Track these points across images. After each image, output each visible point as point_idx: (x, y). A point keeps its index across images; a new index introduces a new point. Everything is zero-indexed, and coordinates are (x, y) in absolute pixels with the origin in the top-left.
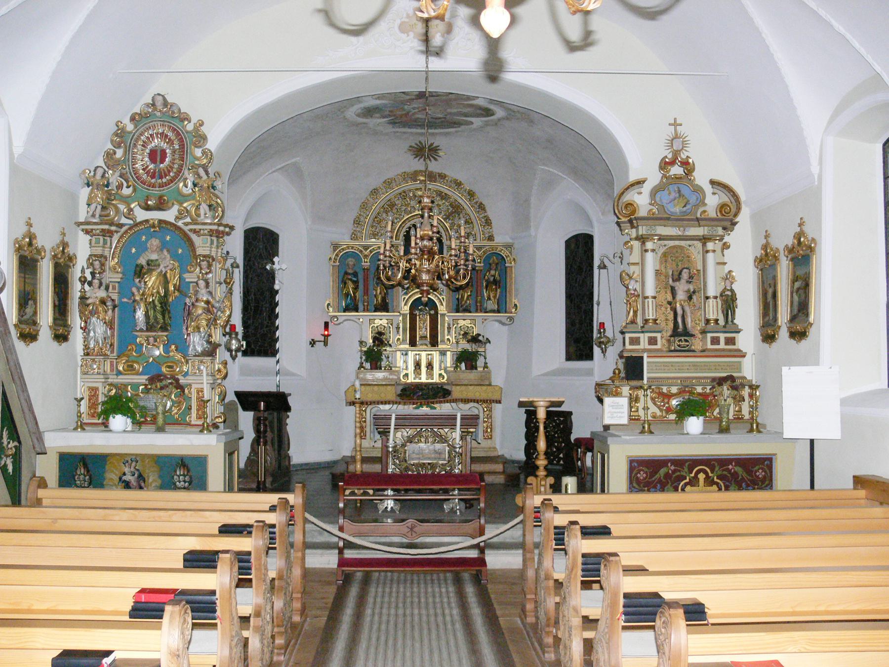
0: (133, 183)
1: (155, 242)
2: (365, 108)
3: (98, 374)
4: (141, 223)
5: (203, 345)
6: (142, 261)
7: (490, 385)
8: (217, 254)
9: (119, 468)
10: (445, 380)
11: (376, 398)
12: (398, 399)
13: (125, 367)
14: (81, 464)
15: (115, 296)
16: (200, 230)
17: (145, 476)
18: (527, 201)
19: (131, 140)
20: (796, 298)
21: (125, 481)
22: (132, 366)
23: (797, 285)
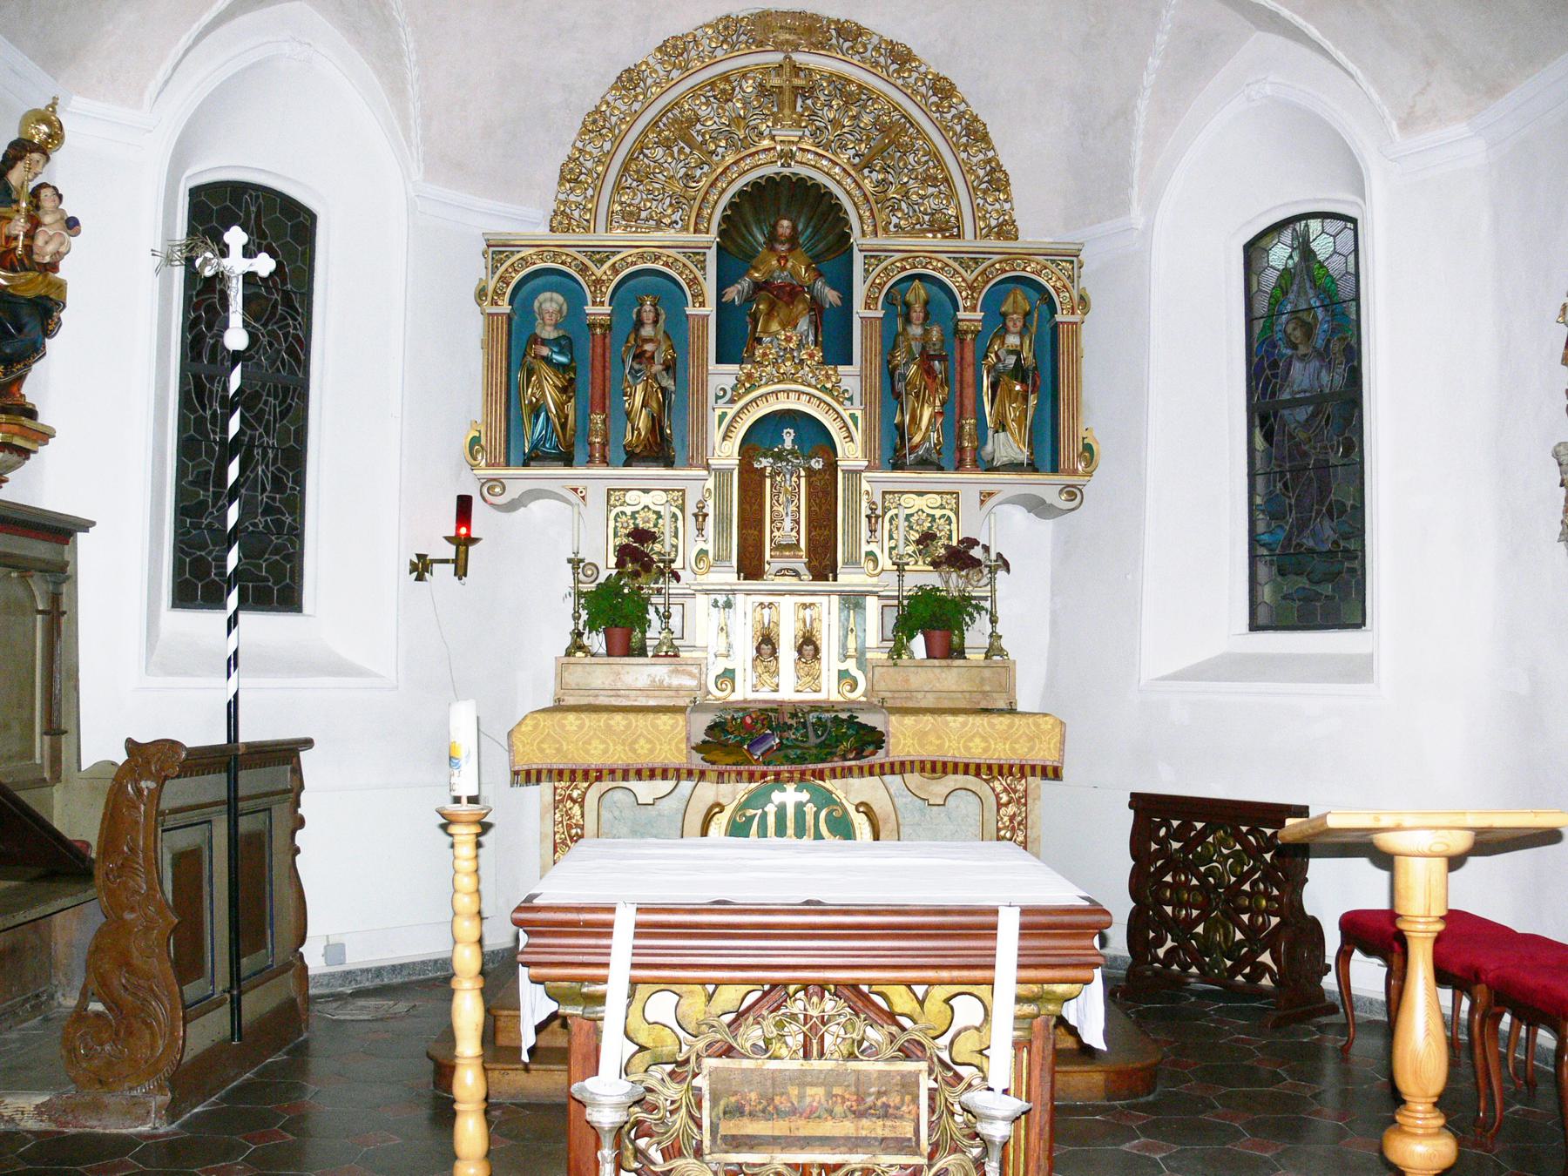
7: (1012, 711)
10: (858, 695)
11: (618, 756)
12: (697, 761)
18: (1125, 114)
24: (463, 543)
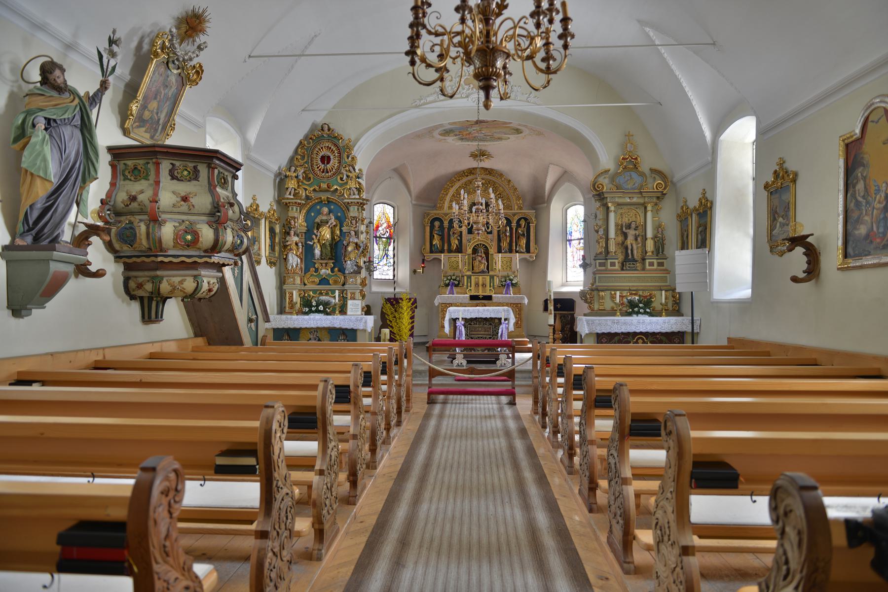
1: (326, 210)
2: (444, 130)
20: (700, 237)
23: (700, 229)
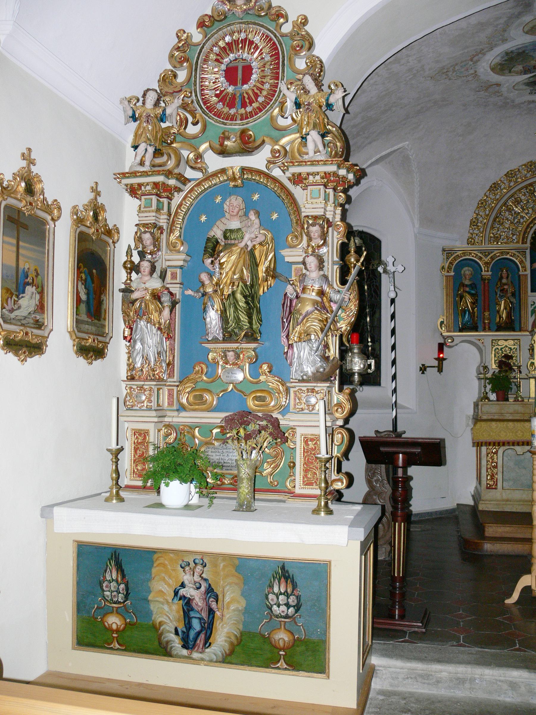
0: (201, 115)
2: (507, 54)
3: (149, 409)
4: (215, 174)
5: (314, 362)
6: (217, 233)
8: (334, 217)
9: (173, 573)
11: (510, 437)
13: (191, 399)
14: (113, 563)
15: (176, 289)
16: (308, 174)
17: (218, 590)
19: (199, 54)
21: (183, 598)
22: (201, 397)
24: (441, 360)
